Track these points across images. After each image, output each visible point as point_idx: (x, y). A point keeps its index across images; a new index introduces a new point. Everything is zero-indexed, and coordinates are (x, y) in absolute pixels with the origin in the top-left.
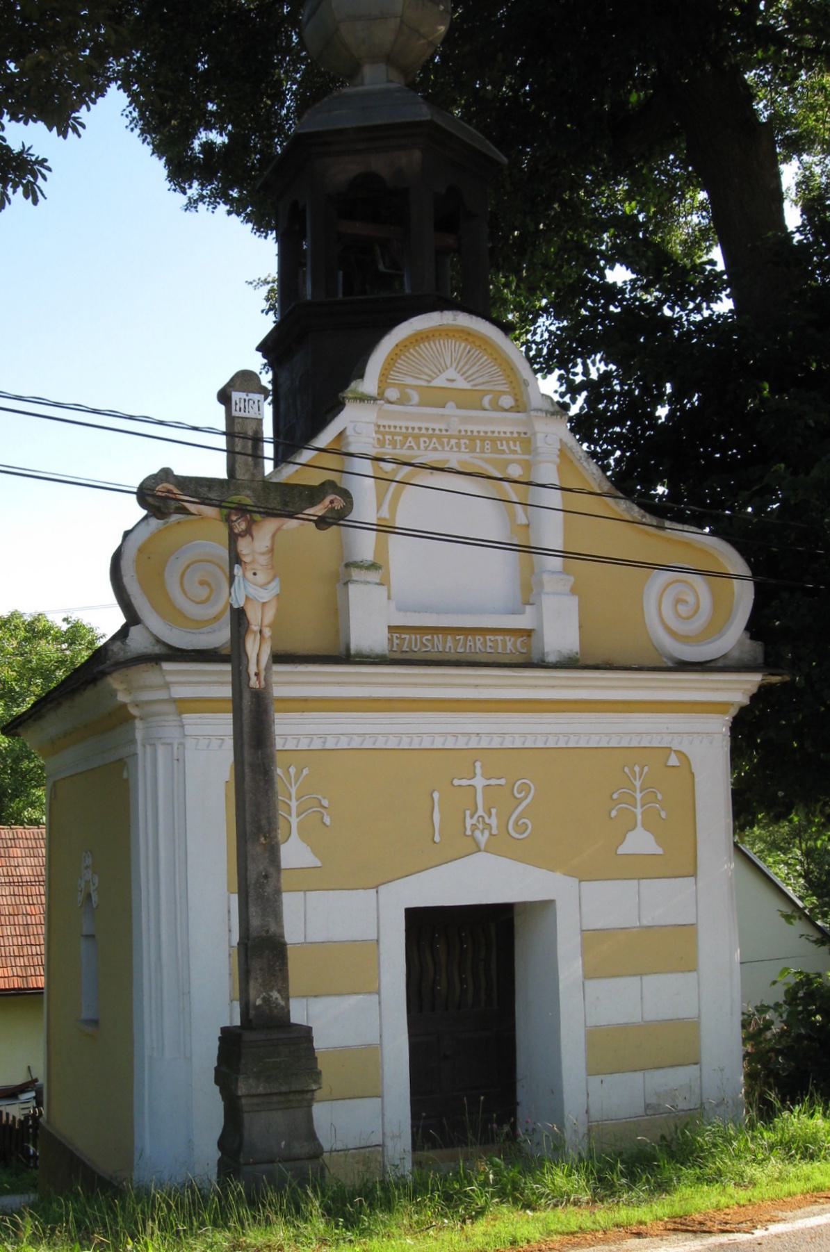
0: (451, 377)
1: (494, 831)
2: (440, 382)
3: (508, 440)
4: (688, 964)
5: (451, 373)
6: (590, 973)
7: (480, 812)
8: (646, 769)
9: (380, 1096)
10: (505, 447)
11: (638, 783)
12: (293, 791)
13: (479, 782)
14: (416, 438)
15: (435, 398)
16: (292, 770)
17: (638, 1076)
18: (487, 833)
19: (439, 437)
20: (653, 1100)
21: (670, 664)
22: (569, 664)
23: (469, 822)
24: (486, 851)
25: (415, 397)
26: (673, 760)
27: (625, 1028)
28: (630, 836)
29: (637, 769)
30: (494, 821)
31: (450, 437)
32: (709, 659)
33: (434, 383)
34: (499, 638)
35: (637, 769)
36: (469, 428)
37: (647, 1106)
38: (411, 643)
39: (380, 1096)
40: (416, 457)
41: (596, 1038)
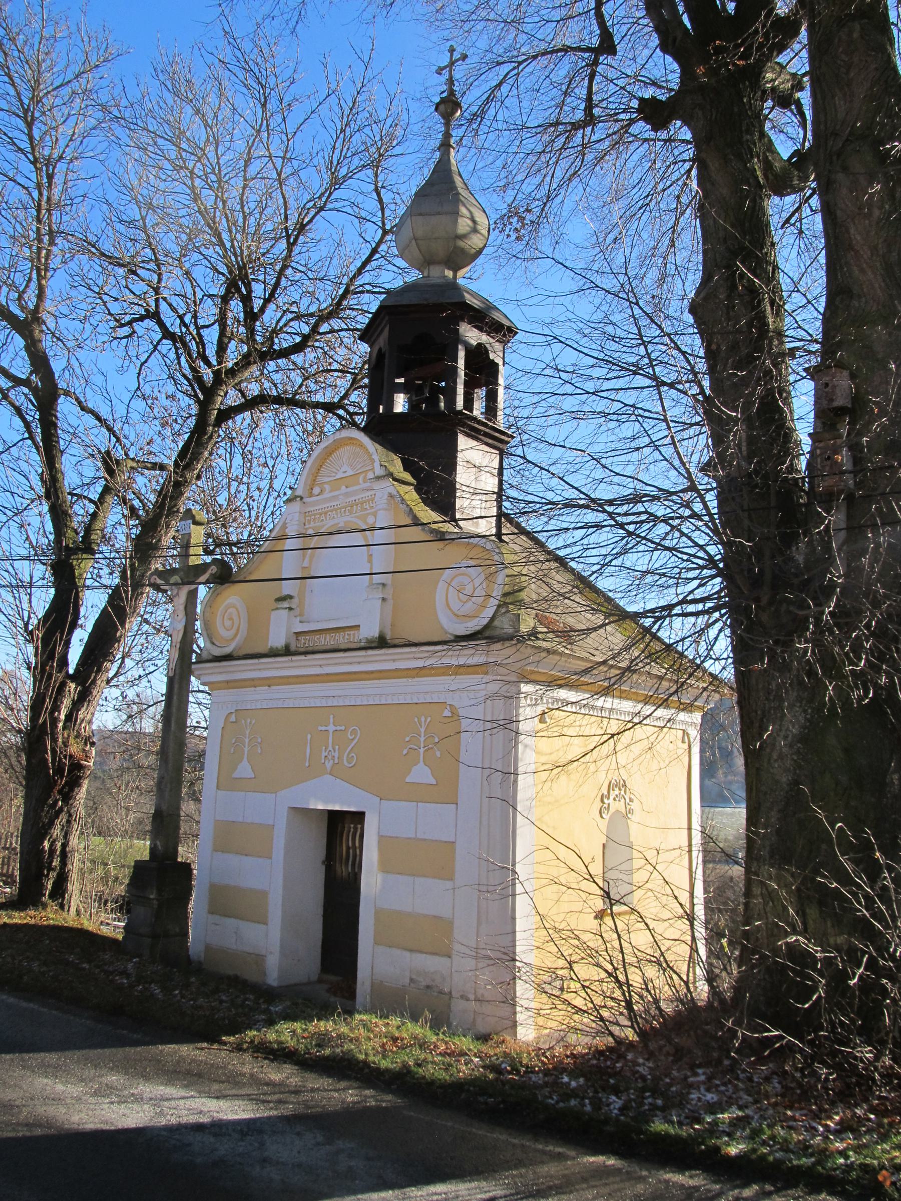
1: (336, 761)
2: (340, 475)
3: (369, 501)
4: (446, 872)
7: (330, 748)
9: (266, 924)
10: (367, 507)
11: (423, 730)
12: (247, 732)
13: (331, 728)
14: (326, 513)
16: (249, 721)
17: (407, 954)
18: (332, 762)
19: (336, 510)
22: (382, 643)
24: (331, 774)
25: (327, 487)
26: (447, 713)
28: (415, 768)
29: (423, 719)
30: (336, 755)
31: (340, 508)
33: (338, 476)
34: (352, 632)
35: (423, 719)
38: (305, 642)
39: (266, 924)
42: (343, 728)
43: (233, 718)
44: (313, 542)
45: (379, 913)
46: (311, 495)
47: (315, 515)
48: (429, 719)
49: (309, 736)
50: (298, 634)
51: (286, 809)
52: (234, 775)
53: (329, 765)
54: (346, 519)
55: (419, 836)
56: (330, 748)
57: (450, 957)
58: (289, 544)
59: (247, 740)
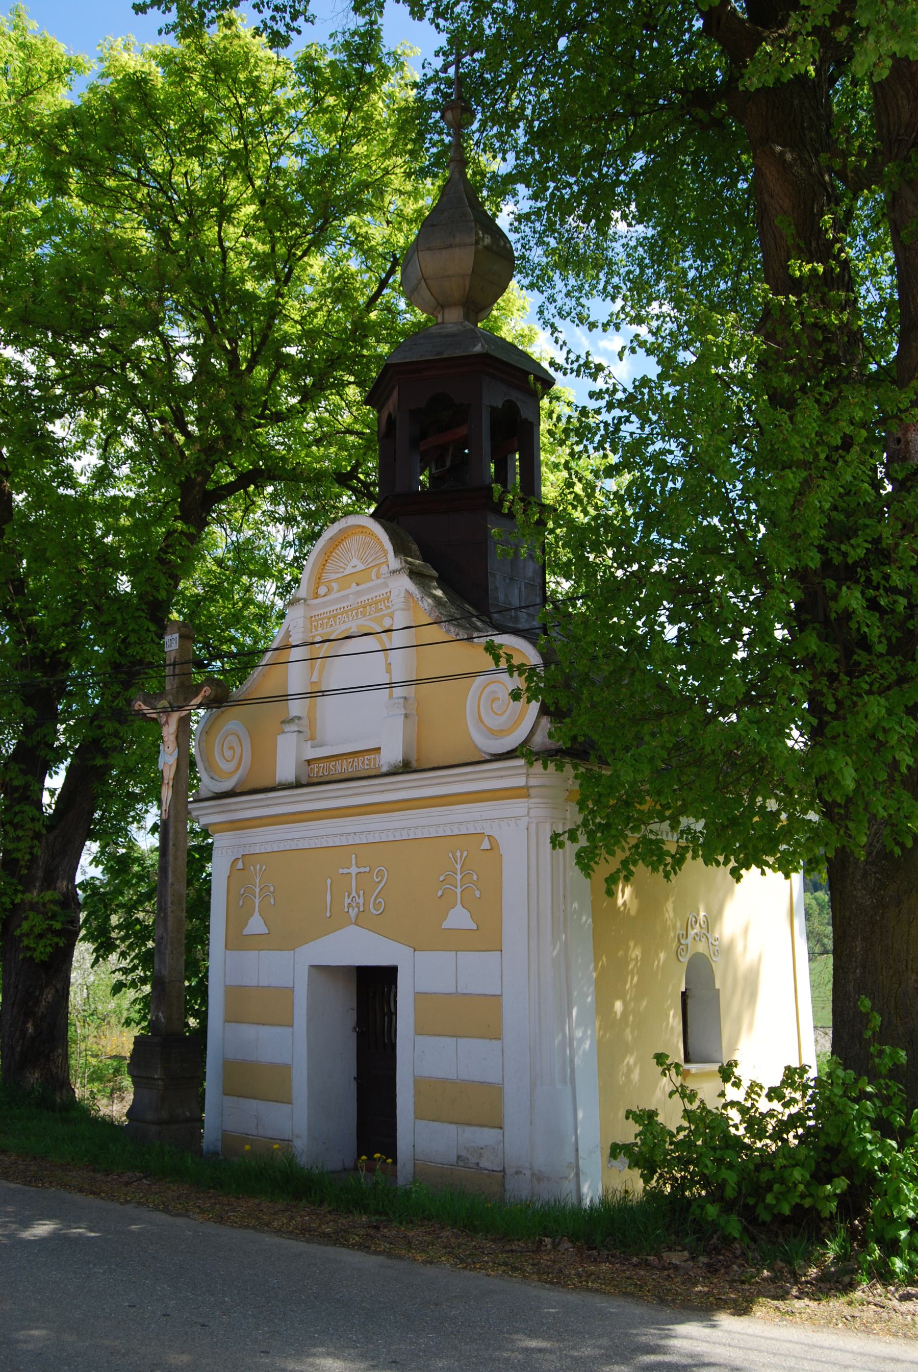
0: (355, 564)
2: (349, 570)
4: (493, 1032)
5: (355, 561)
6: (420, 1031)
7: (354, 894)
8: (465, 854)
11: (458, 867)
13: (354, 870)
15: (344, 582)
17: (453, 1127)
20: (464, 1153)
21: (488, 757)
22: (406, 768)
23: (347, 901)
24: (356, 924)
25: (335, 586)
27: (444, 1081)
28: (452, 912)
29: (458, 854)
30: (361, 901)
32: (509, 749)
35: (458, 854)
36: (363, 599)
37: (459, 1157)
38: (318, 771)
40: (333, 632)
41: (421, 1084)
42: (367, 869)
43: (240, 865)
44: (324, 649)
45: (419, 1082)
46: (316, 595)
47: (322, 619)
48: (465, 854)
49: (329, 881)
50: (309, 762)
51: (307, 968)
52: (246, 932)
53: (353, 913)
54: (361, 622)
55: (460, 990)
56: (354, 894)
57: (501, 1128)
58: (295, 654)
59: (257, 890)
